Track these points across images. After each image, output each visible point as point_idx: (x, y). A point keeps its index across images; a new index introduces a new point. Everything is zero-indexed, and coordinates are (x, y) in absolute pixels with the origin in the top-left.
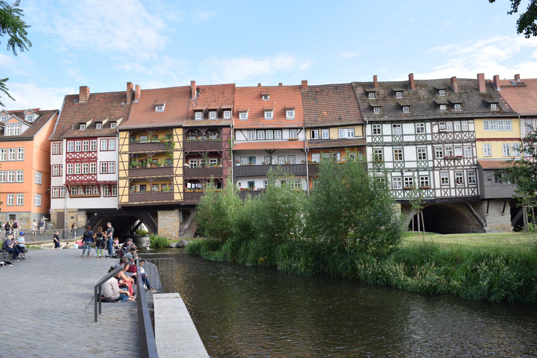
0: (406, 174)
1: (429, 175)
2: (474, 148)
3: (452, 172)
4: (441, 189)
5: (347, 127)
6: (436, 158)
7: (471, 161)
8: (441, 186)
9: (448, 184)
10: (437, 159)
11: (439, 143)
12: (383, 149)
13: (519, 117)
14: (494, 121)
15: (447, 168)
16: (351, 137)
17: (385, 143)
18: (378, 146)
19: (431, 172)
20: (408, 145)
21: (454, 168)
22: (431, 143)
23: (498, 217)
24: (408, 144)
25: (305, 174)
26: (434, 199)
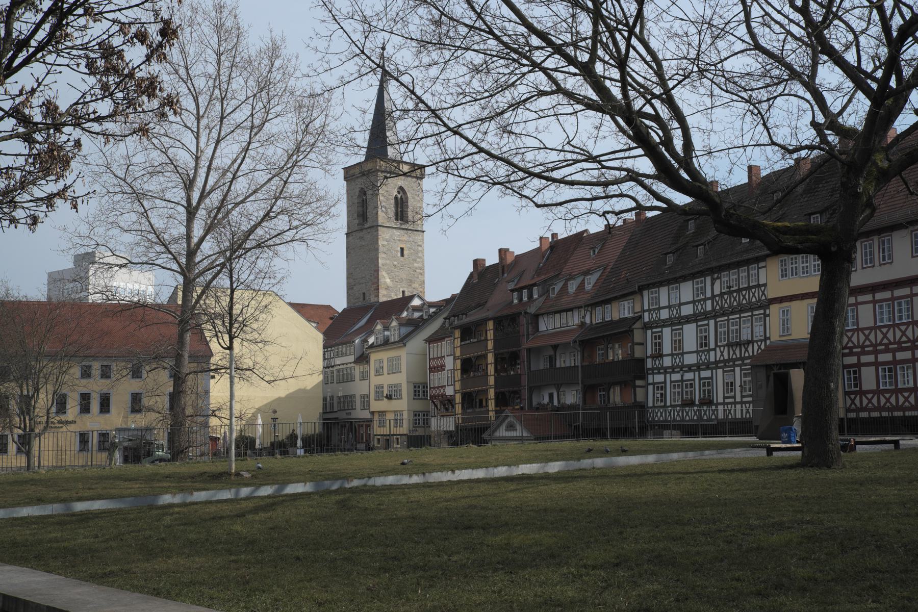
0: (689, 376)
1: (711, 378)
2: (767, 319)
3: (738, 370)
4: (724, 404)
5: (628, 298)
6: (719, 344)
7: (763, 347)
8: (725, 398)
9: (732, 394)
10: (720, 347)
11: (723, 315)
12: (661, 332)
15: (731, 363)
16: (631, 315)
17: (664, 320)
18: (657, 327)
19: (714, 371)
21: (740, 362)
22: (714, 315)
24: (688, 320)
26: (715, 422)
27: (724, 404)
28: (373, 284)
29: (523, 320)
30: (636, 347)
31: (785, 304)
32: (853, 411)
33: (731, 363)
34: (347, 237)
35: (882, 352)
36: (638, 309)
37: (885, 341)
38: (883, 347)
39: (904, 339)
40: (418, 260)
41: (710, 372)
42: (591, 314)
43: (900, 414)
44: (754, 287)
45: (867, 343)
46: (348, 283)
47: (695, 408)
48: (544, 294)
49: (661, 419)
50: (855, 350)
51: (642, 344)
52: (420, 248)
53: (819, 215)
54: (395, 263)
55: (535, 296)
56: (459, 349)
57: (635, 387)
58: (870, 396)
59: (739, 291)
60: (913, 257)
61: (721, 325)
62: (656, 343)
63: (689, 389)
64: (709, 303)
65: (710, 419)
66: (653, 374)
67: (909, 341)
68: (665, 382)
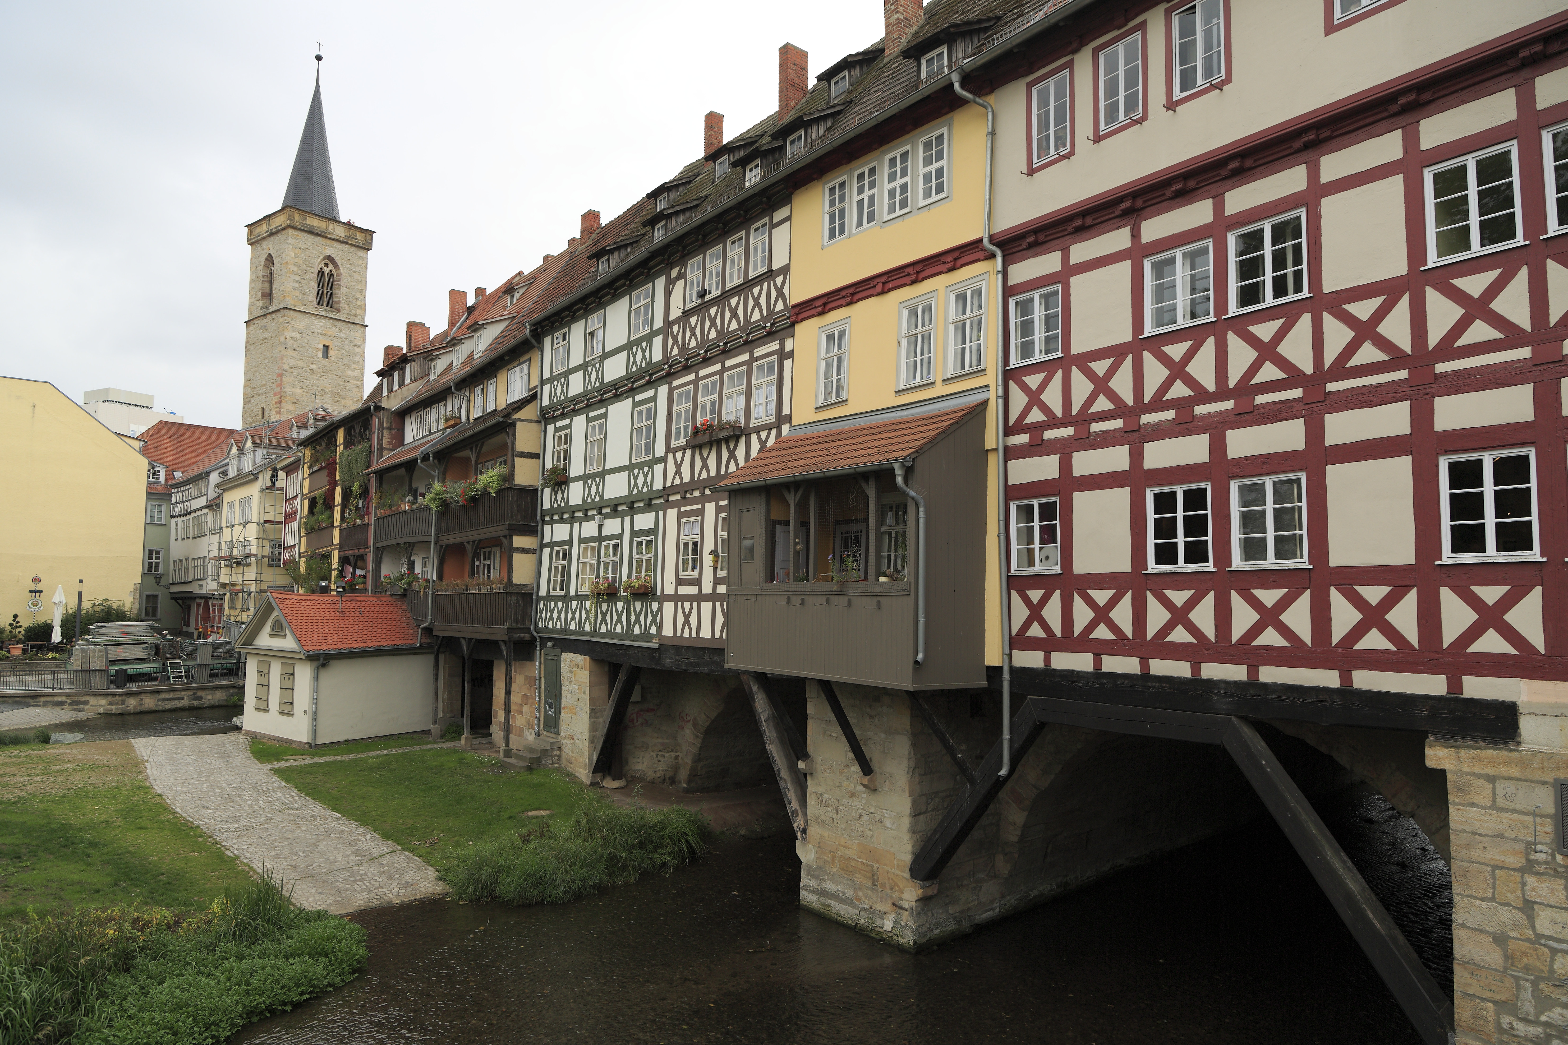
0: (612, 526)
2: (787, 363)
4: (676, 598)
5: (522, 360)
6: (674, 444)
7: (770, 443)
8: (679, 582)
11: (687, 369)
12: (569, 426)
13: (957, 86)
14: (872, 171)
16: (525, 394)
18: (563, 416)
20: (617, 397)
23: (853, 795)
25: (426, 539)
27: (676, 598)
28: (275, 395)
29: (376, 422)
30: (519, 461)
31: (834, 316)
32: (1033, 644)
33: (697, 494)
34: (247, 326)
35: (1159, 432)
36: (535, 382)
37: (1180, 390)
38: (1170, 414)
39: (1269, 372)
40: (353, 366)
41: (652, 515)
42: (469, 401)
43: (1237, 673)
44: (758, 280)
45: (1102, 404)
46: (245, 394)
47: (620, 605)
48: (422, 378)
49: (558, 626)
50: (1049, 435)
51: (536, 456)
52: (357, 350)
53: (945, 49)
54: (313, 367)
55: (407, 381)
56: (307, 482)
57: (510, 551)
58: (1101, 596)
59: (726, 295)
60: (1331, 28)
61: (680, 395)
62: (559, 453)
63: (611, 558)
64: (658, 341)
65: (645, 636)
66: (552, 522)
67: (1294, 377)
68: (569, 542)
